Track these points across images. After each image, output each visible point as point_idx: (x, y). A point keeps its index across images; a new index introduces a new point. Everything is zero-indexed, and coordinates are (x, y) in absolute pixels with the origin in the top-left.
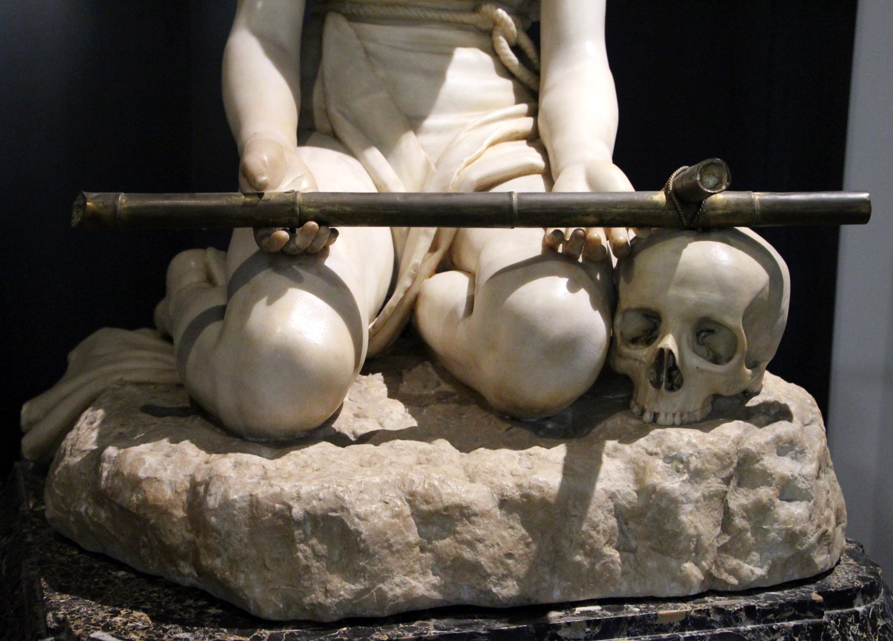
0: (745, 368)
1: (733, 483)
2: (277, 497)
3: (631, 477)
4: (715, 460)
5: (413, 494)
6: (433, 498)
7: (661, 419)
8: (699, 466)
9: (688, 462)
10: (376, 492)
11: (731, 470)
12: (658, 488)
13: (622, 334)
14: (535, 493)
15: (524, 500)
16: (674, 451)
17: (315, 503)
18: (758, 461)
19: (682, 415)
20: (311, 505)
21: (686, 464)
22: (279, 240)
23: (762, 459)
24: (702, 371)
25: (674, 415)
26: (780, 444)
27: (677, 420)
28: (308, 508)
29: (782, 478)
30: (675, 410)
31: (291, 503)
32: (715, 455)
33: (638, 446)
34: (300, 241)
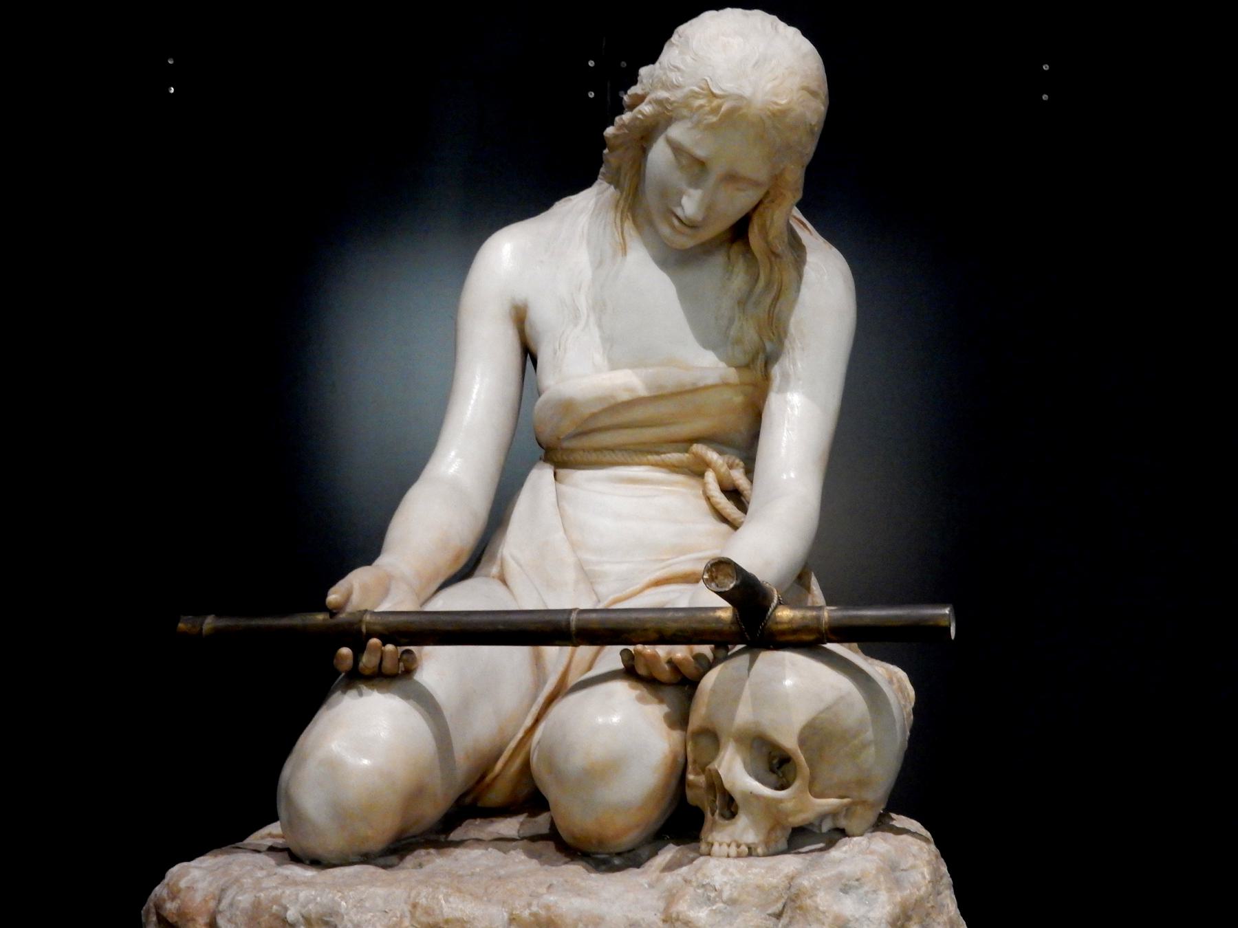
0: (812, 798)
1: (784, 920)
2: (276, 900)
3: (662, 905)
4: (757, 892)
5: (415, 906)
6: (433, 910)
7: (716, 848)
8: (735, 894)
9: (721, 891)
10: (380, 902)
11: (779, 906)
12: (681, 917)
13: (695, 762)
14: (543, 913)
15: (532, 918)
16: (708, 877)
17: (311, 906)
18: (811, 897)
19: (738, 846)
20: (306, 909)
21: (720, 893)
22: (345, 657)
23: (816, 895)
24: (758, 797)
25: (729, 845)
26: (844, 881)
27: (733, 850)
28: (303, 911)
29: (837, 918)
30: (728, 840)
31: (288, 906)
32: (758, 887)
33: (678, 874)
34: (368, 661)
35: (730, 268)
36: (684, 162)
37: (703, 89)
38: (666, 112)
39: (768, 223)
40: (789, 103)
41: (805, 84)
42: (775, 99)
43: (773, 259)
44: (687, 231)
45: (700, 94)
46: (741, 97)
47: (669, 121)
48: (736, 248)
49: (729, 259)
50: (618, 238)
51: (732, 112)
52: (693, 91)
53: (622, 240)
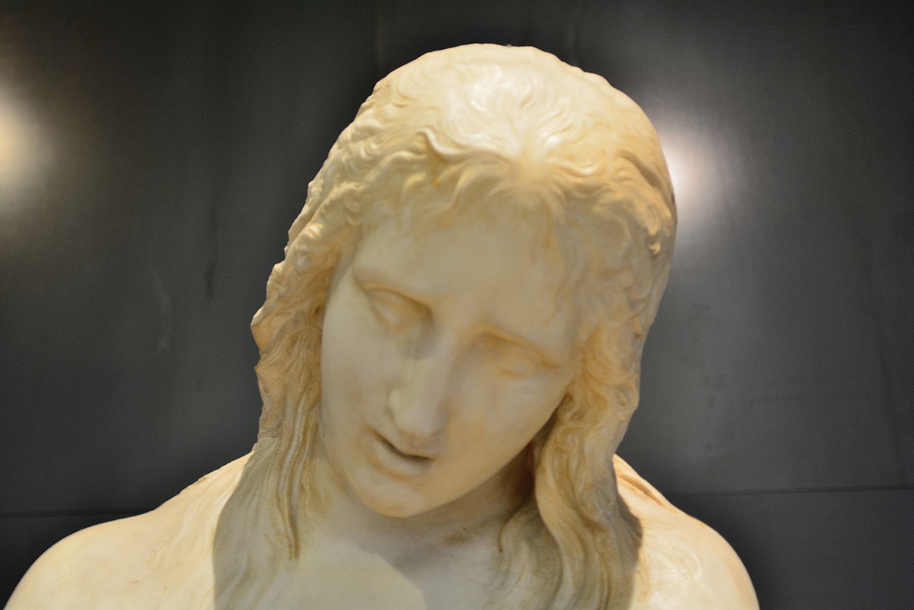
35: (504, 567)
36: (392, 316)
37: (416, 151)
38: (350, 221)
39: (574, 464)
40: (600, 173)
41: (629, 149)
42: (567, 164)
43: (588, 537)
44: (404, 467)
45: (413, 162)
46: (496, 158)
47: (358, 236)
48: (514, 529)
49: (501, 550)
50: (283, 525)
51: (483, 185)
52: (399, 162)
53: (289, 529)
